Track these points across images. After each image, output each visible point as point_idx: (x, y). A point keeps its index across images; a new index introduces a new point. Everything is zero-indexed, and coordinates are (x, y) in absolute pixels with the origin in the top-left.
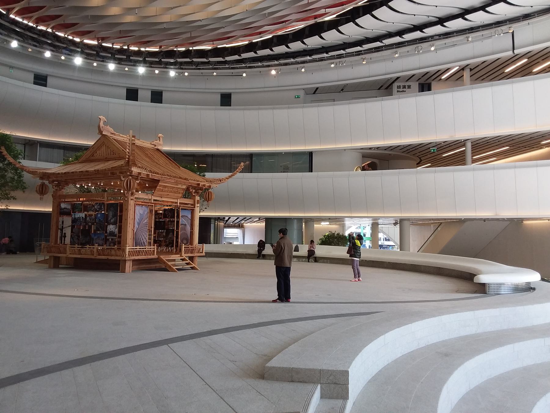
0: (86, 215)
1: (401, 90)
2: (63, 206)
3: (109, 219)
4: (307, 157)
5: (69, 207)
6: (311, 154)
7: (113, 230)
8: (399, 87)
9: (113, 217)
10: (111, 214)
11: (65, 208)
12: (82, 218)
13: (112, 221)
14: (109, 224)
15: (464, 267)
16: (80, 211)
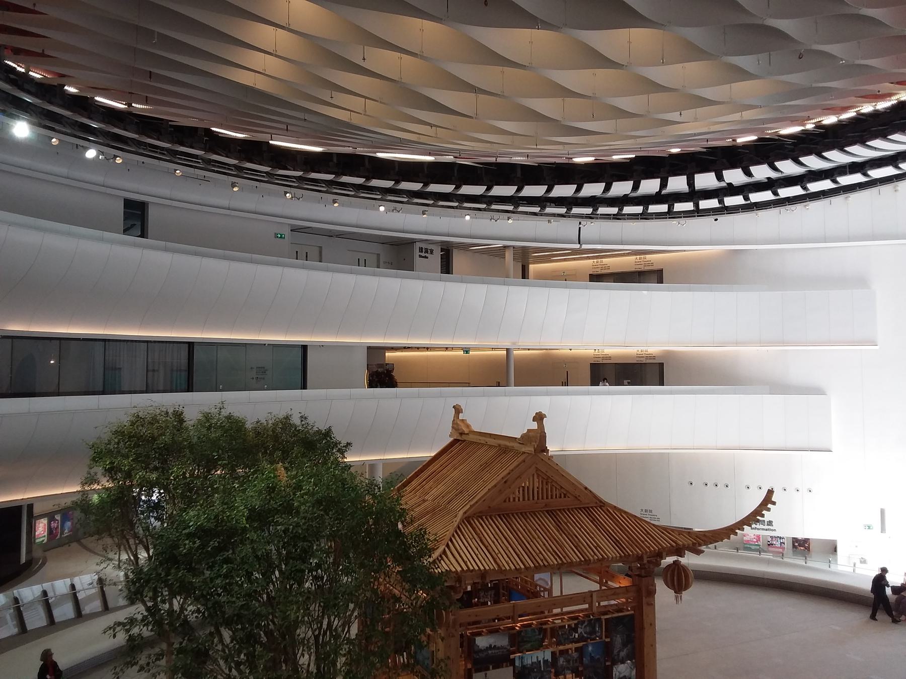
0: (553, 654)
1: (423, 254)
2: (482, 642)
3: (615, 652)
4: (299, 353)
5: (502, 641)
6: (304, 348)
7: (627, 674)
8: (421, 250)
9: (624, 645)
10: (618, 640)
11: (490, 647)
12: (546, 662)
13: (622, 654)
14: (614, 663)
15: (784, 575)
16: (539, 646)
